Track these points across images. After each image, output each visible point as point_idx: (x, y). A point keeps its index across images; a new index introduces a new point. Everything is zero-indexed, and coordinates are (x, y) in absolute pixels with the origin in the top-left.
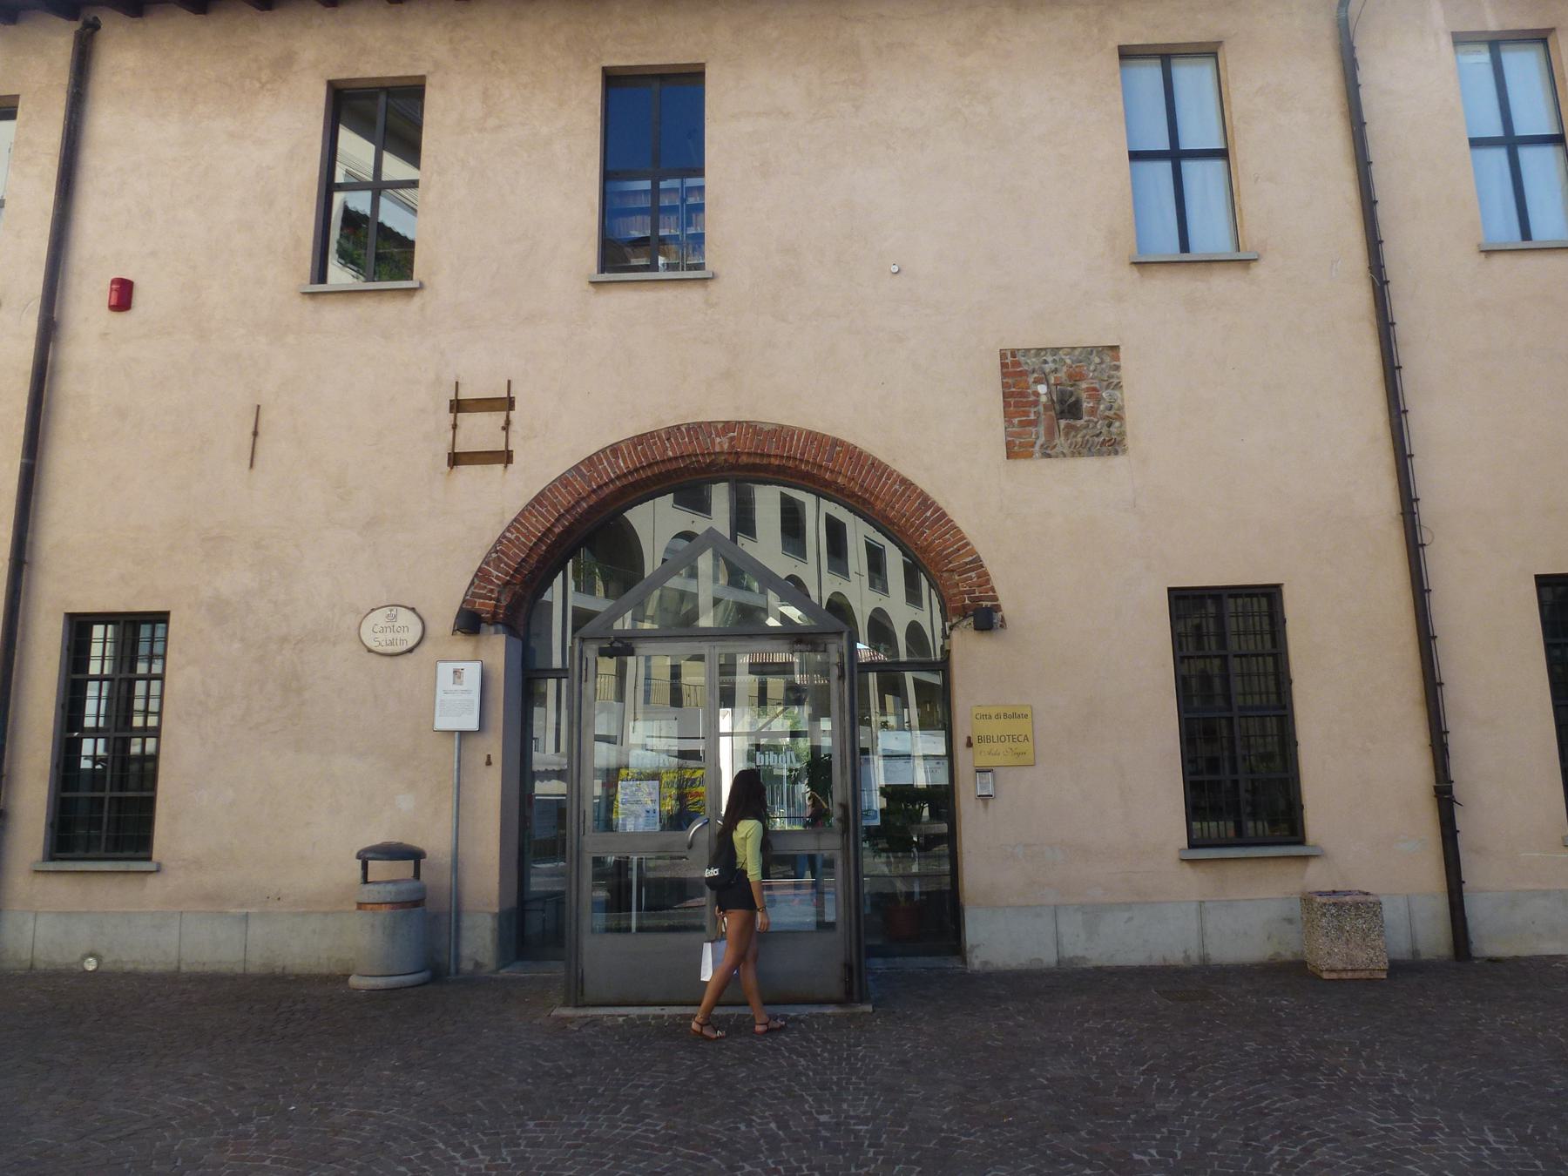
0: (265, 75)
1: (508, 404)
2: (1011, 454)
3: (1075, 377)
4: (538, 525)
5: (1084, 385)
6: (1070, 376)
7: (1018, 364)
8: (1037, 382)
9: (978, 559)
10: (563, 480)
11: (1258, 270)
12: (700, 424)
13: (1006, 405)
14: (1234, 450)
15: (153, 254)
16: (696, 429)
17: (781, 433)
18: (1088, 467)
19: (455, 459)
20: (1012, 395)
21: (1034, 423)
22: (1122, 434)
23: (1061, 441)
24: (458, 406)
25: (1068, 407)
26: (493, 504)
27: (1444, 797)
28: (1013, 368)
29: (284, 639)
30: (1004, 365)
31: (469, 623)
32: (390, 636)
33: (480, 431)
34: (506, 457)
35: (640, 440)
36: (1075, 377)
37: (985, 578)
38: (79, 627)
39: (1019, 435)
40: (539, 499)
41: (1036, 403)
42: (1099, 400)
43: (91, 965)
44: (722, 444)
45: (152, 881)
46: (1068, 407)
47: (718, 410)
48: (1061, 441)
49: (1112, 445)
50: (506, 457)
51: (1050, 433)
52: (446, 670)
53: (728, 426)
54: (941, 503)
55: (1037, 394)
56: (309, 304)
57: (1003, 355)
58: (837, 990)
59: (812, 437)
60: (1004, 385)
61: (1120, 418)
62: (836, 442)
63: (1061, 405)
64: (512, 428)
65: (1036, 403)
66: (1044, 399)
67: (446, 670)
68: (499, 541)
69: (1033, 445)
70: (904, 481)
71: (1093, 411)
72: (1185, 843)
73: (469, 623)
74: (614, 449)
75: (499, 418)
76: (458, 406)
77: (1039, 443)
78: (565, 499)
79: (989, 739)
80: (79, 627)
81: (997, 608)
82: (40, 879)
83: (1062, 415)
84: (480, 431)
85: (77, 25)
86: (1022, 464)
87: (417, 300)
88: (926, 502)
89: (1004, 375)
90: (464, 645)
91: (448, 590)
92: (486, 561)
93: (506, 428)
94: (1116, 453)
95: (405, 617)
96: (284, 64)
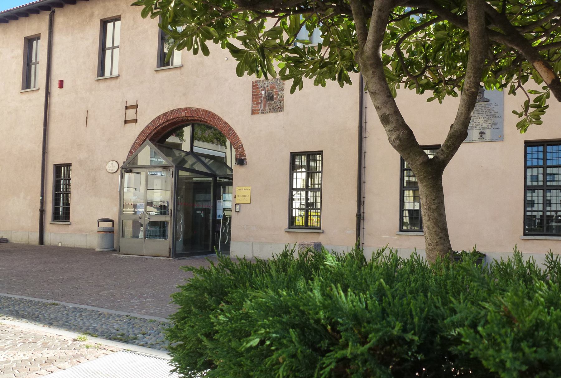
0: (88, 20)
1: (137, 106)
3: (272, 88)
5: (274, 90)
6: (271, 88)
7: (257, 85)
8: (262, 90)
9: (242, 145)
10: (148, 126)
12: (179, 109)
13: (253, 98)
15: (67, 73)
16: (178, 110)
17: (197, 110)
18: (273, 115)
19: (126, 122)
20: (255, 95)
21: (260, 103)
22: (283, 105)
23: (267, 108)
25: (270, 98)
27: (360, 217)
29: (92, 170)
30: (253, 86)
32: (111, 168)
33: (131, 114)
34: (136, 121)
35: (165, 114)
36: (272, 88)
37: (243, 150)
38: (58, 168)
39: (256, 107)
40: (143, 132)
41: (261, 97)
42: (278, 95)
43: (60, 245)
44: (183, 114)
45: (70, 226)
46: (270, 98)
47: (182, 105)
50: (136, 121)
51: (265, 106)
54: (234, 129)
55: (262, 94)
56: (97, 83)
57: (253, 83)
58: (168, 255)
60: (253, 92)
61: (283, 100)
62: (210, 112)
64: (138, 113)
65: (261, 97)
66: (263, 96)
68: (134, 143)
69: (259, 110)
70: (226, 123)
71: (276, 98)
72: (287, 227)
74: (159, 117)
75: (134, 110)
76: (127, 108)
77: (262, 109)
78: (148, 131)
79: (239, 196)
80: (58, 168)
81: (245, 159)
82: (51, 225)
83: (268, 100)
84: (131, 114)
85: (49, 12)
86: (256, 116)
87: (119, 80)
88: (231, 129)
89: (253, 89)
92: (131, 149)
93: (136, 113)
94: (281, 111)
95: (115, 163)
96: (92, 15)
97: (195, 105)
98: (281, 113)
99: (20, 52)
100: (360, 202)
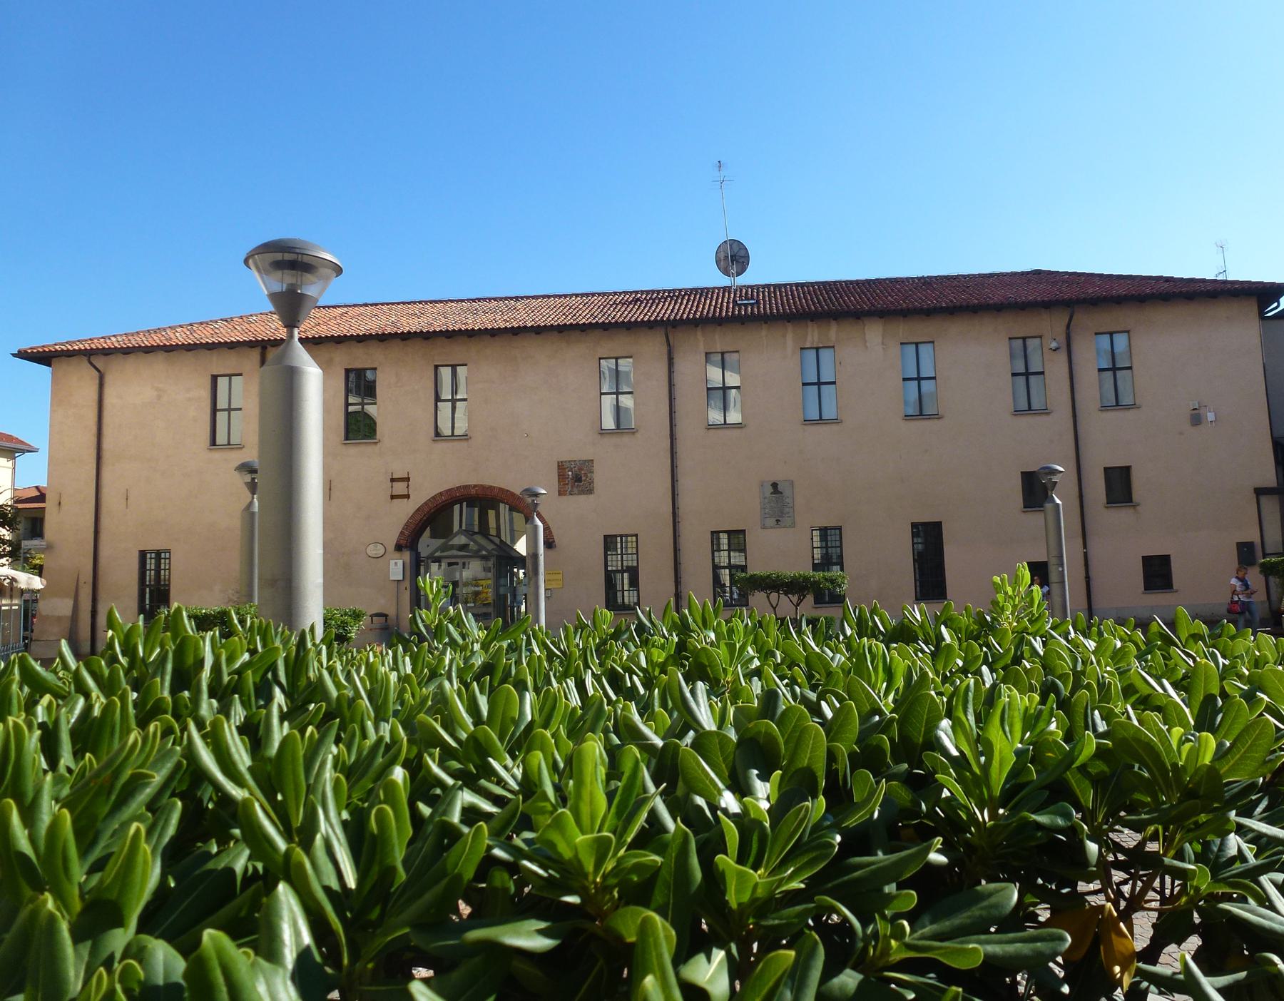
1: (408, 479)
2: (560, 494)
3: (580, 469)
4: (418, 518)
10: (426, 503)
11: (638, 435)
14: (629, 492)
18: (583, 498)
19: (393, 497)
23: (576, 490)
24: (393, 480)
25: (578, 479)
26: (404, 511)
28: (561, 467)
31: (399, 548)
33: (400, 488)
34: (408, 496)
36: (580, 469)
46: (578, 479)
47: (472, 481)
48: (576, 490)
49: (590, 491)
50: (408, 496)
52: (392, 562)
53: (475, 486)
59: (500, 489)
63: (575, 478)
67: (392, 562)
73: (399, 548)
76: (393, 480)
78: (426, 509)
84: (400, 488)
90: (397, 555)
91: (392, 538)
97: (488, 482)
98: (591, 496)
99: (205, 394)
100: (677, 582)
